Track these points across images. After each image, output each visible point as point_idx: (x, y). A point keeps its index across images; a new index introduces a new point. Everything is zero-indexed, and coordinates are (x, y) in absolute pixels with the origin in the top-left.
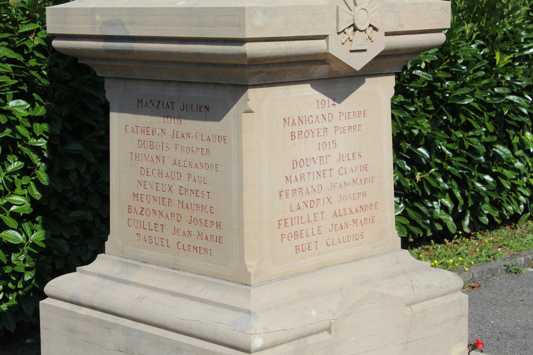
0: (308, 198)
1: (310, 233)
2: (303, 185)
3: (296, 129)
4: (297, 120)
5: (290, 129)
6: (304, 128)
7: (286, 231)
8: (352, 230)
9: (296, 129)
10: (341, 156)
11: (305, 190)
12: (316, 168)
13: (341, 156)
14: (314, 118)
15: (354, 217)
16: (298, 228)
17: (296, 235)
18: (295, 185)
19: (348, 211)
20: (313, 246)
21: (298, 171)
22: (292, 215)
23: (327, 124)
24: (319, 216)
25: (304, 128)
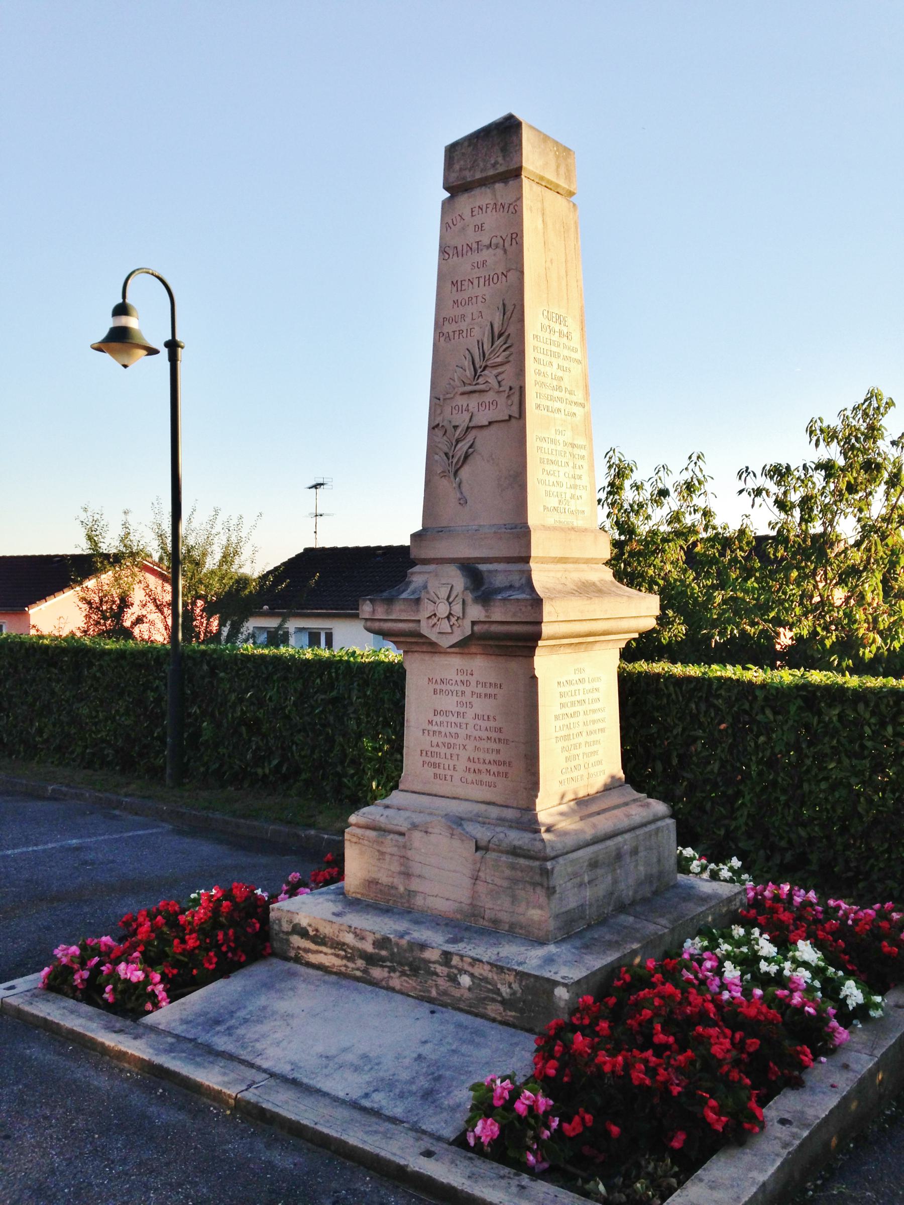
0: (447, 740)
1: (446, 767)
2: (443, 729)
3: (438, 687)
4: (439, 681)
5: (432, 687)
6: (444, 687)
7: (427, 759)
8: (486, 778)
9: (438, 687)
10: (476, 716)
11: (443, 734)
12: (454, 719)
13: (476, 716)
14: (454, 682)
15: (488, 767)
16: (437, 761)
17: (435, 765)
18: (436, 728)
19: (482, 761)
20: (448, 778)
21: (438, 719)
22: (433, 749)
23: (464, 688)
24: (455, 757)
25: (444, 687)
